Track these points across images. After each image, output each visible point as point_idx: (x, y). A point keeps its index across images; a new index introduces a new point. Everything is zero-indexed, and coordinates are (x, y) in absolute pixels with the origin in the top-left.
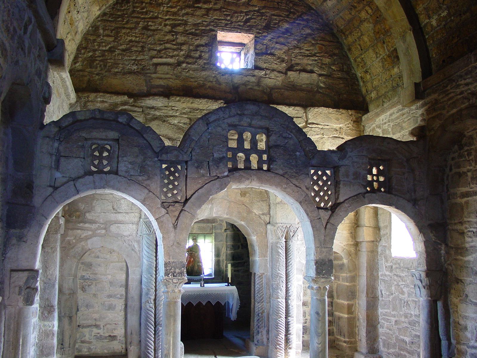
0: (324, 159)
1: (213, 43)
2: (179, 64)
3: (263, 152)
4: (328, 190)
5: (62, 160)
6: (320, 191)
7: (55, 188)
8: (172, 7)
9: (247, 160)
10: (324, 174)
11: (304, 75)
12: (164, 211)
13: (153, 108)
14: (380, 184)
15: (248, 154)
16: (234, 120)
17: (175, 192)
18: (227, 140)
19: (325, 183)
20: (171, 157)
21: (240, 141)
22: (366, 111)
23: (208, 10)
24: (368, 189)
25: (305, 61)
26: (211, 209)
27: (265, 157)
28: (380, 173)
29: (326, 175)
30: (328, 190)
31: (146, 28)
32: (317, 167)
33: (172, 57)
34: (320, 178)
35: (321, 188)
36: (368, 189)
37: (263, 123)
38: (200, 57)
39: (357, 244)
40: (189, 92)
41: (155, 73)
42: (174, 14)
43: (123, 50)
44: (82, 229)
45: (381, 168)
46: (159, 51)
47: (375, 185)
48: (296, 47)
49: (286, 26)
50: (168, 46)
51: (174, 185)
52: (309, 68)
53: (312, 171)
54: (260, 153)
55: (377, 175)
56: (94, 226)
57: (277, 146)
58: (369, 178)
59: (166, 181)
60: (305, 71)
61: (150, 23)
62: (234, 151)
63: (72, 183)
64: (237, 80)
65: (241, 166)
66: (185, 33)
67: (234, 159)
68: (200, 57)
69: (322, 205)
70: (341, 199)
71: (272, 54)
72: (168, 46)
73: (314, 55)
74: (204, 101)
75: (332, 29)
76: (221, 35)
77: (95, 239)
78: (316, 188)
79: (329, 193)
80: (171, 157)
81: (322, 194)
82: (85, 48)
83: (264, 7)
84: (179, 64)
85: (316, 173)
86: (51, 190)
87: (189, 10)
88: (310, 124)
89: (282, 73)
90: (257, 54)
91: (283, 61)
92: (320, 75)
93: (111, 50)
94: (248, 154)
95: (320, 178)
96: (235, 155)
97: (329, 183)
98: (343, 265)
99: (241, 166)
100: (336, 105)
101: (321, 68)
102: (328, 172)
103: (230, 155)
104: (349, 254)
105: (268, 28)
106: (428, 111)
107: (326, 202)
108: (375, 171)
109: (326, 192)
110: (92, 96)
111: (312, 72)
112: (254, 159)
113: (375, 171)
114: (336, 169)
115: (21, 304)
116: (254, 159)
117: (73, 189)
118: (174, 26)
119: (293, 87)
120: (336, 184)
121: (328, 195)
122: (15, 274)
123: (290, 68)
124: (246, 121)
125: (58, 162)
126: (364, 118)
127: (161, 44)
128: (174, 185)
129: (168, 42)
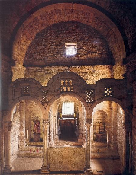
0: (90, 87)
1: (64, 48)
2: (54, 55)
3: (72, 86)
4: (92, 97)
5: (15, 92)
6: (89, 97)
7: (14, 100)
8: (51, 37)
9: (67, 89)
10: (91, 91)
11: (93, 54)
12: (42, 105)
13: (47, 70)
14: (110, 94)
15: (67, 86)
16: (62, 77)
17: (46, 99)
18: (60, 83)
19: (91, 94)
20: (44, 89)
21: (64, 83)
22: (114, 64)
23: (62, 36)
24: (106, 95)
25: (94, 49)
26: (65, 98)
27: (72, 87)
28: (110, 90)
29: (91, 92)
30: (92, 97)
31: (44, 45)
32: (88, 90)
33: (52, 53)
34: (89, 93)
35: (89, 96)
36: (106, 95)
37: (70, 77)
38: (60, 53)
39: (111, 109)
40: (58, 64)
41: (47, 59)
42: (52, 39)
43: (38, 53)
44: (31, 105)
45: (111, 88)
46: (48, 52)
47: (108, 94)
48: (90, 45)
49: (87, 38)
50: (51, 50)
51: (46, 97)
52: (95, 52)
53: (87, 91)
54: (70, 86)
55: (109, 91)
56: (33, 104)
57: (75, 84)
58: (106, 92)
59: (44, 96)
60: (93, 53)
61: (45, 43)
62: (63, 86)
63: (18, 99)
64: (72, 59)
65: (65, 90)
66: (56, 45)
67: (63, 89)
68: (60, 53)
69: (90, 101)
70: (95, 100)
71: (83, 49)
72: (51, 50)
73: (97, 47)
74: (61, 67)
75: (103, 37)
76: (66, 44)
77: (34, 108)
78: (88, 96)
79: (92, 97)
80: (44, 89)
81: (90, 98)
82: (28, 53)
83: (80, 33)
84: (54, 55)
85: (88, 91)
86: (13, 101)
87: (57, 38)
88: (94, 71)
89: (86, 54)
90: (78, 49)
91: (86, 50)
92: (99, 54)
93: (35, 53)
94: (67, 86)
95: (89, 93)
96: (63, 88)
97: (92, 94)
98: (107, 115)
99: (65, 90)
100: (104, 63)
101: (99, 51)
102: (92, 91)
103: (61, 87)
104: (109, 111)
105: (81, 40)
106: (127, 69)
107: (91, 100)
108: (108, 90)
109: (91, 97)
110: (30, 68)
111: (96, 53)
112: (69, 88)
113: (108, 90)
114: (94, 90)
115: (7, 130)
116: (69, 88)
117: (18, 100)
118: (52, 43)
119: (89, 59)
120: (94, 96)
121: (92, 98)
122: (5, 123)
123: (88, 53)
124: (65, 77)
125: (15, 93)
126: (114, 67)
127: (49, 50)
128: (46, 97)
129: (50, 49)
